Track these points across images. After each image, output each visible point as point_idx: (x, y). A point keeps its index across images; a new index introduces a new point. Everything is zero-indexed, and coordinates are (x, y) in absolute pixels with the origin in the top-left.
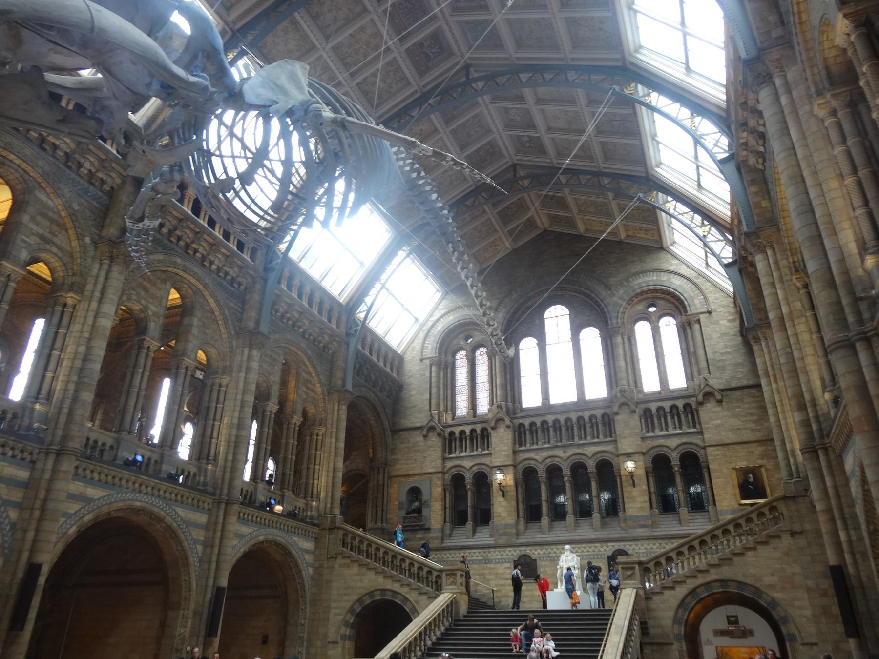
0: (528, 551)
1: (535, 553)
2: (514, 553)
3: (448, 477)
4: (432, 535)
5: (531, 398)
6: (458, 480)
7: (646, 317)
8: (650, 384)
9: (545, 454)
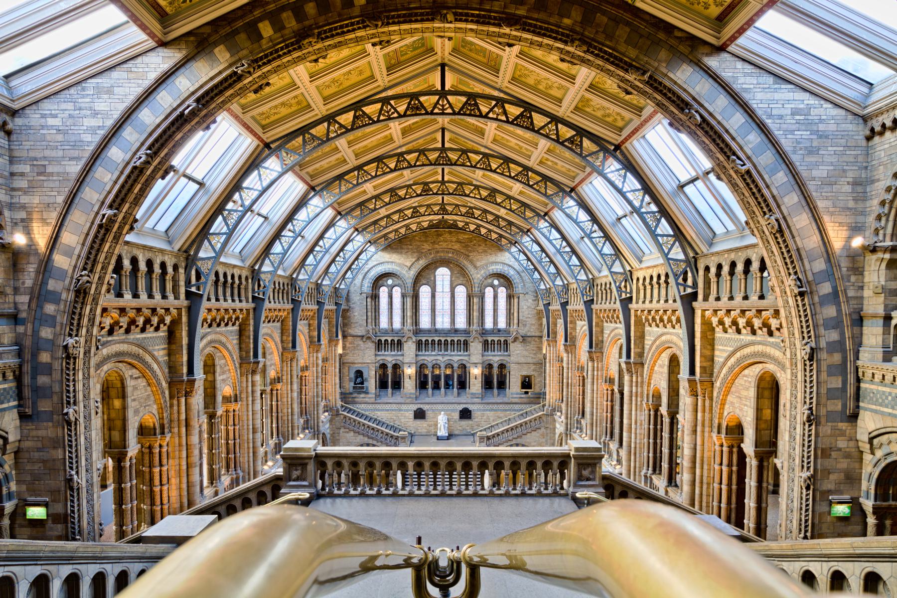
0: (421, 406)
1: (425, 407)
2: (415, 407)
3: (378, 365)
4: (370, 396)
5: (425, 322)
6: (383, 366)
7: (492, 286)
8: (489, 324)
9: (433, 358)
